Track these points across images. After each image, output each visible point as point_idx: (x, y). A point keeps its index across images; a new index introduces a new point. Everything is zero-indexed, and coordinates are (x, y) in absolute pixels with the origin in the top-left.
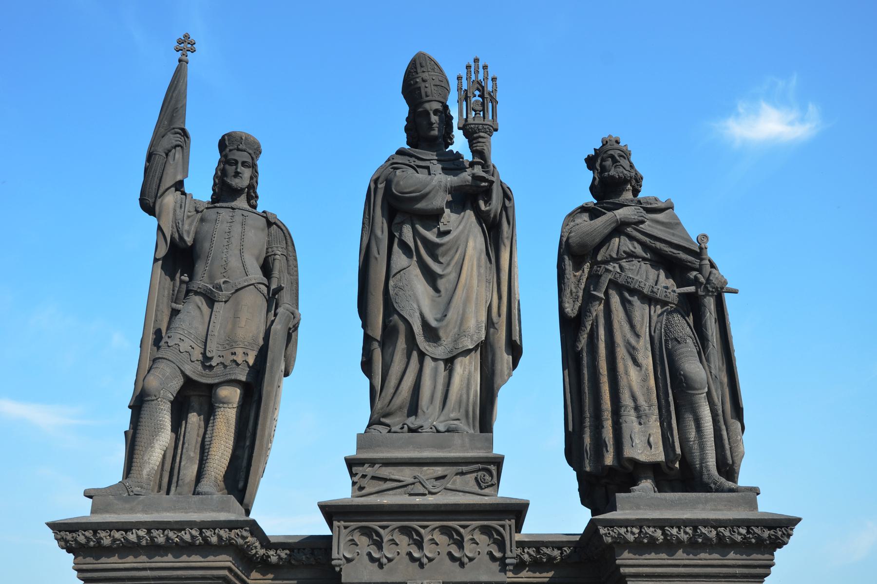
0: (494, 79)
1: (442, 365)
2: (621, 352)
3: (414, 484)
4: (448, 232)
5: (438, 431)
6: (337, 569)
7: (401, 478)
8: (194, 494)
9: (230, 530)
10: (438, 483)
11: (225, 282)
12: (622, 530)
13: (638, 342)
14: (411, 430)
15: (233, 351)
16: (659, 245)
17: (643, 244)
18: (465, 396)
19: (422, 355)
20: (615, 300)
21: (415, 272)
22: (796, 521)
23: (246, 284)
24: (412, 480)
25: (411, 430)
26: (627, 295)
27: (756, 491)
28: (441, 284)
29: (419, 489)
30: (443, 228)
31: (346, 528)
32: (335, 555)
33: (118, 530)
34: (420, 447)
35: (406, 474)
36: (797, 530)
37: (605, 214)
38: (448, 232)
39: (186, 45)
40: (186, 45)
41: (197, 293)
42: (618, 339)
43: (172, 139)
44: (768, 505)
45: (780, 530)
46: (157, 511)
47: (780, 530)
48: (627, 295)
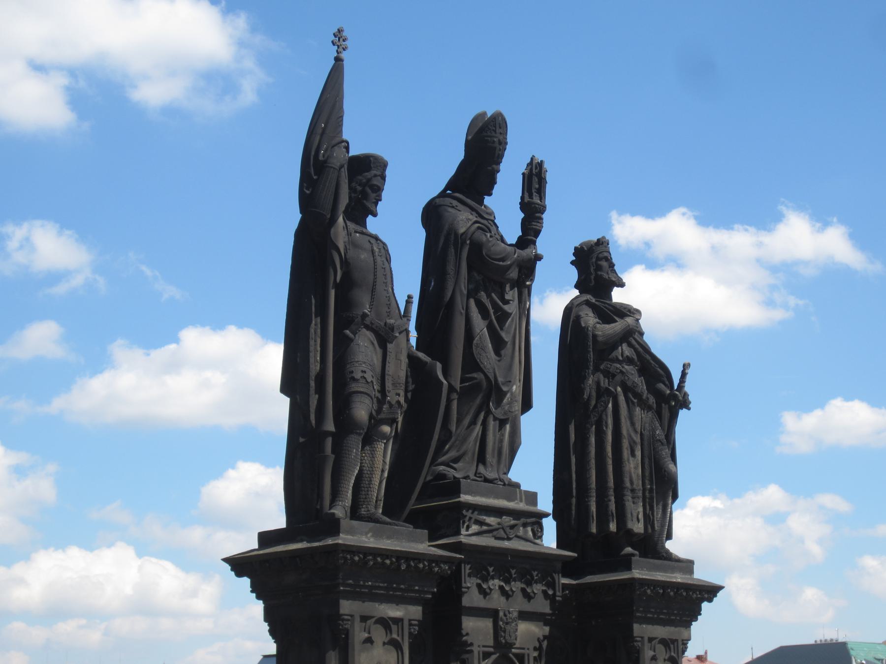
1: (497, 422)
2: (625, 444)
14: (486, 480)
20: (622, 399)
24: (498, 526)
25: (486, 480)
26: (630, 395)
27: (691, 562)
29: (501, 533)
32: (464, 585)
35: (492, 520)
36: (720, 594)
37: (616, 321)
39: (339, 37)
40: (339, 37)
41: (368, 328)
45: (710, 591)
47: (710, 591)
48: (630, 395)
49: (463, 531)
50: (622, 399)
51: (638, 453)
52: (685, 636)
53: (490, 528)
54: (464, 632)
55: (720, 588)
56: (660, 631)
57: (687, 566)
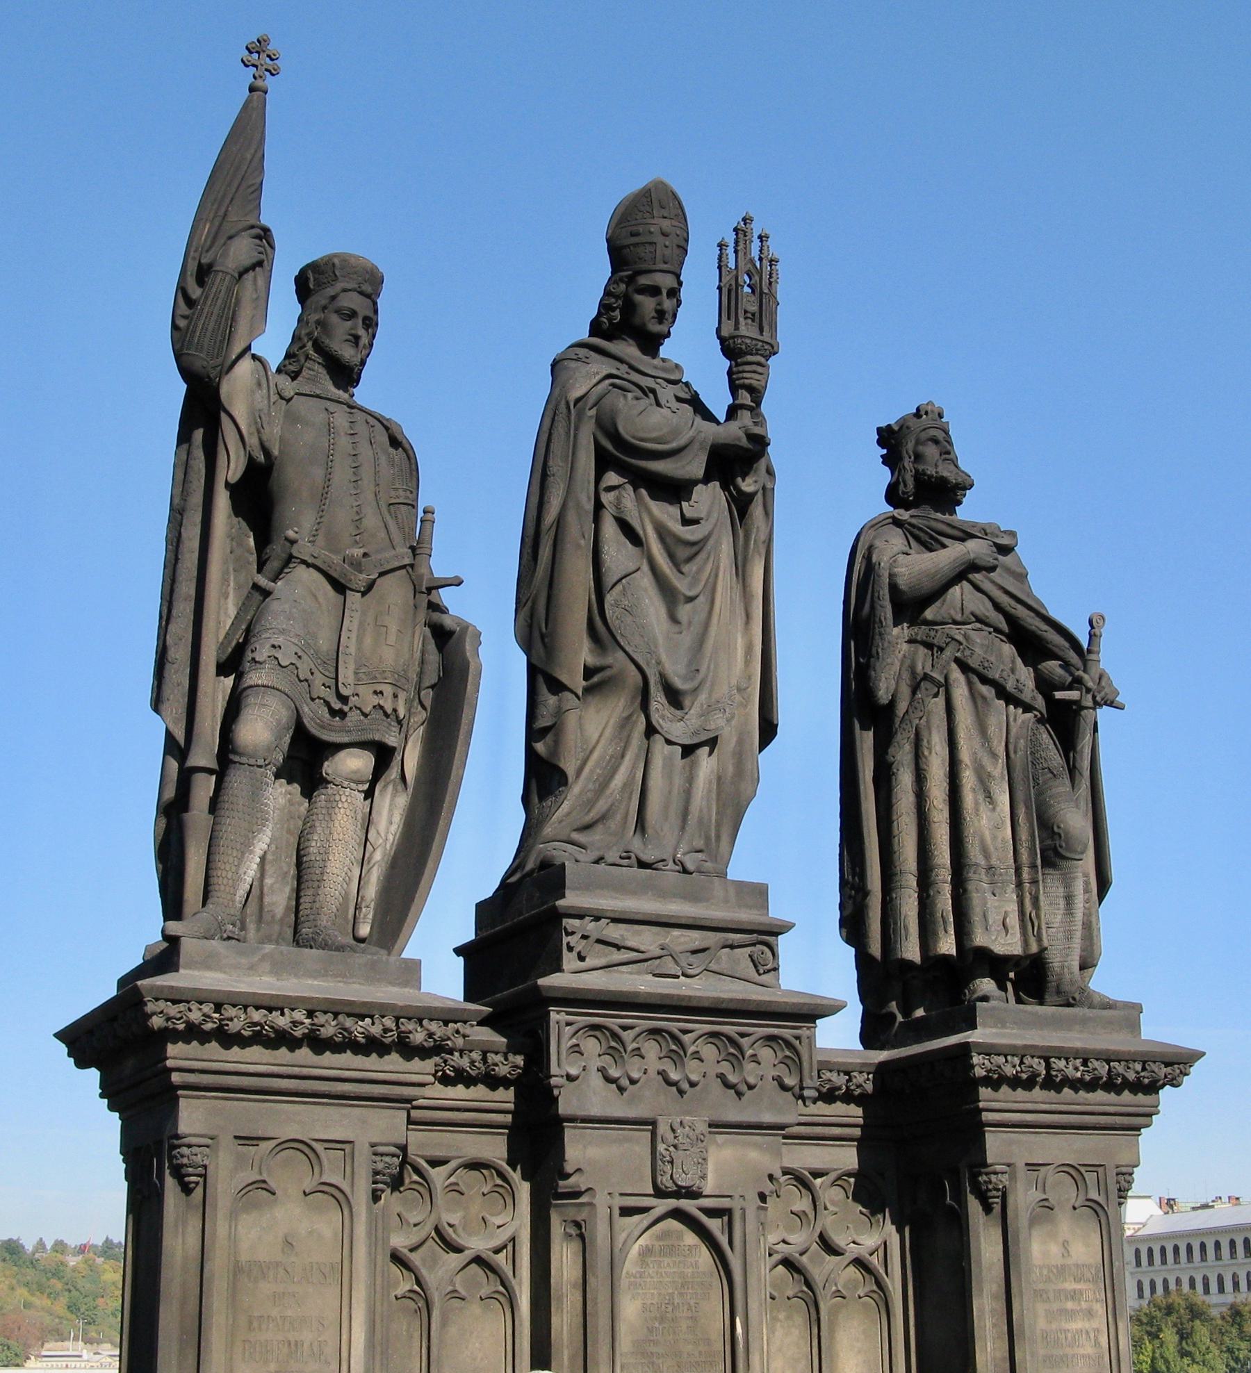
0: (772, 262)
2: (968, 778)
3: (660, 957)
4: (695, 522)
5: (685, 871)
6: (556, 1092)
7: (642, 948)
8: (298, 940)
9: (446, 1023)
10: (692, 958)
11: (365, 555)
12: (1001, 1059)
13: (995, 764)
14: (642, 865)
15: (379, 688)
16: (1021, 611)
17: (997, 607)
18: (705, 811)
19: (651, 731)
20: (960, 692)
21: (645, 580)
22: (1199, 1055)
23: (397, 564)
24: (658, 952)
25: (642, 865)
28: (684, 611)
30: (689, 513)
31: (568, 1024)
32: (554, 1069)
33: (257, 1008)
34: (663, 894)
35: (647, 939)
38: (695, 522)
42: (965, 755)
43: (242, 250)
44: (1158, 1030)
45: (1177, 1064)
46: (296, 976)
47: (1177, 1064)
49: (569, 961)
50: (960, 692)
51: (1004, 799)
52: (1124, 1158)
53: (642, 956)
54: (569, 1168)
55: (1199, 1055)
56: (1060, 1148)
57: (1130, 1015)
